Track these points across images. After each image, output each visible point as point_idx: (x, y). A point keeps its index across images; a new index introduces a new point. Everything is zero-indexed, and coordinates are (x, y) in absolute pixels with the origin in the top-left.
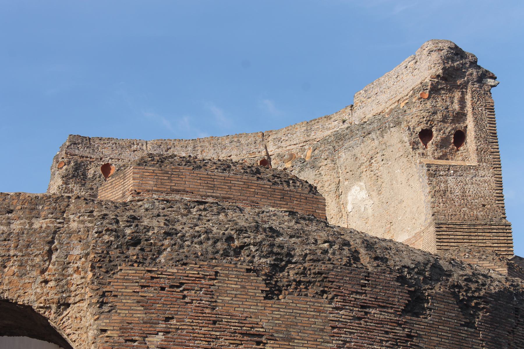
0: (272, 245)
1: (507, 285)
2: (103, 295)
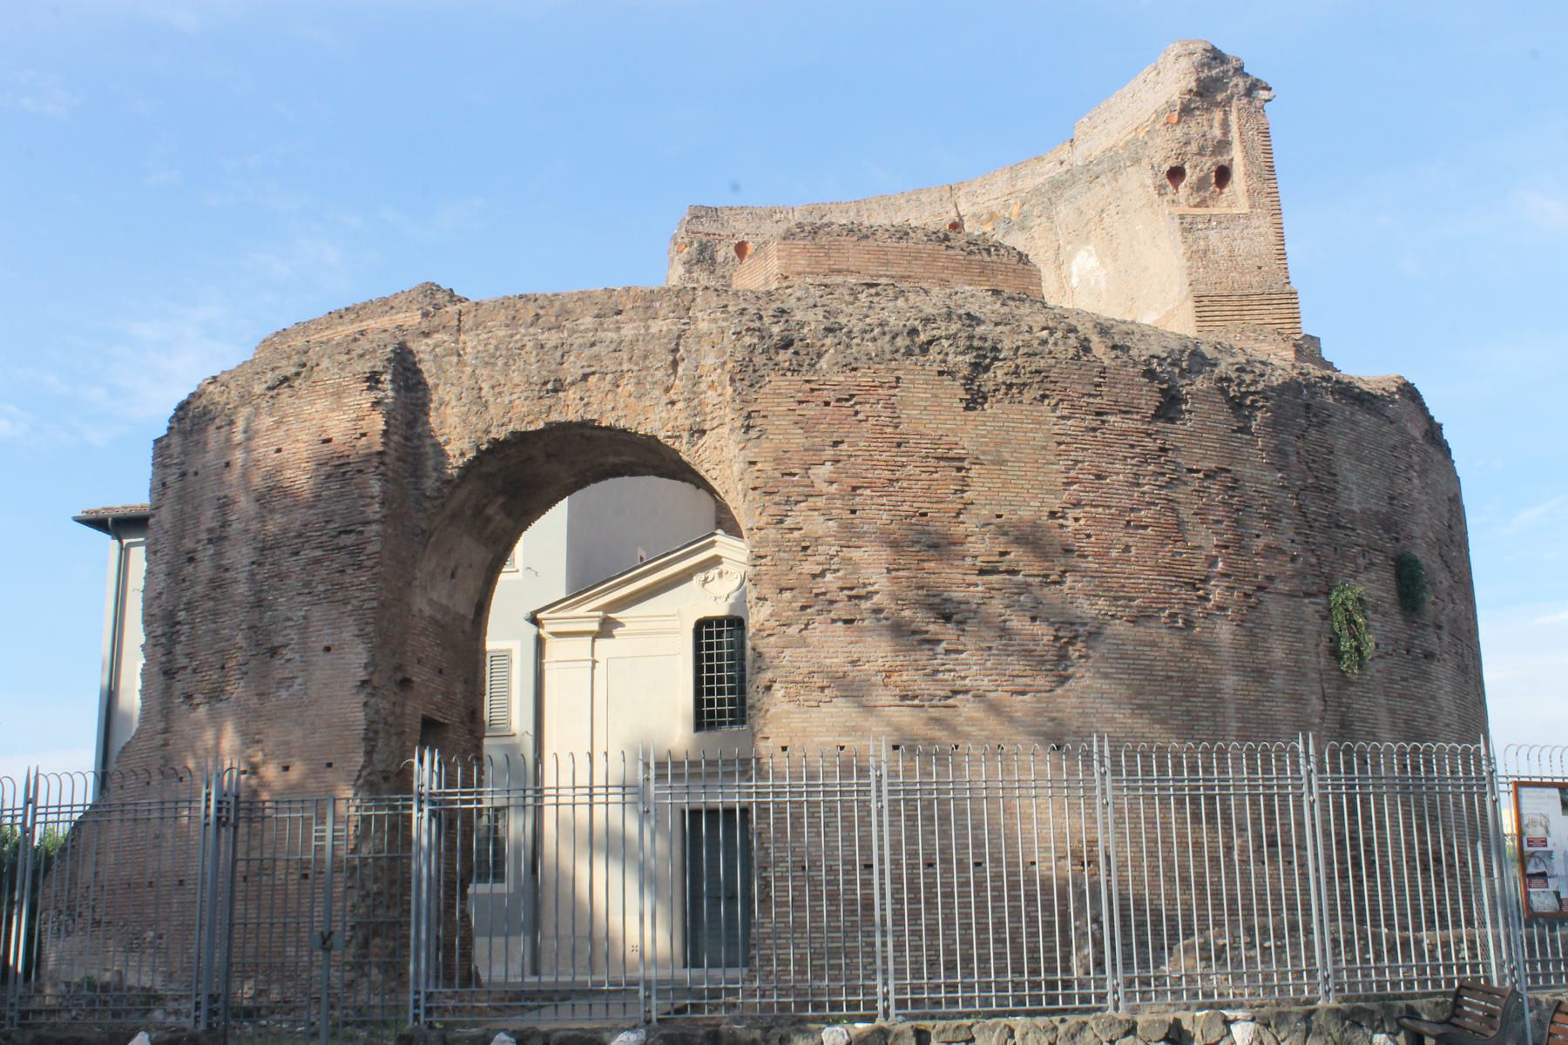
0: (971, 337)
1: (1294, 373)
2: (749, 416)
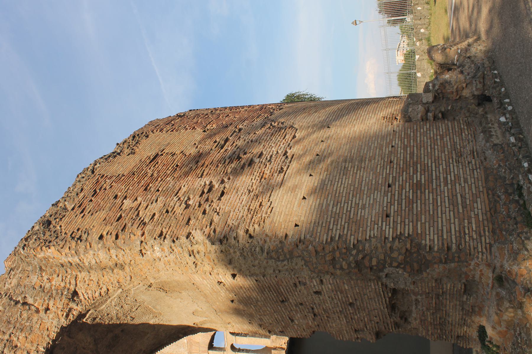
2: (73, 238)
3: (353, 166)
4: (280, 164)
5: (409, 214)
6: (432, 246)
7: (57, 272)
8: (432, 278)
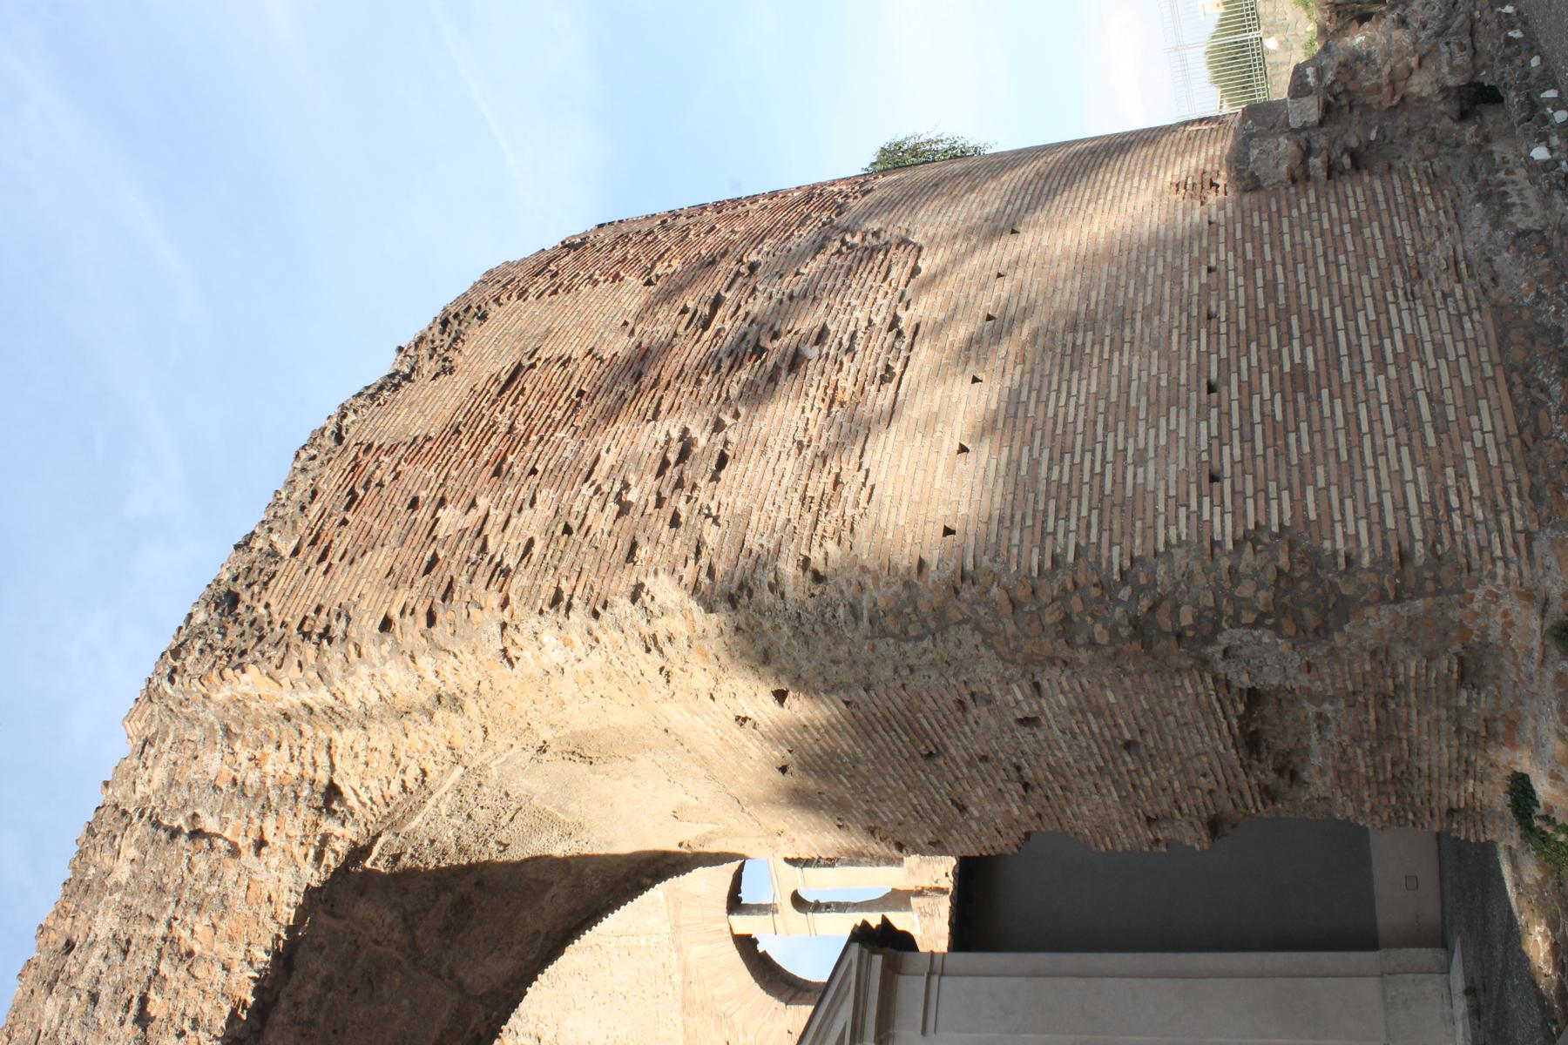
2: (306, 635)
3: (1098, 339)
4: (882, 356)
5: (1277, 468)
6: (1354, 553)
7: (275, 736)
8: (1362, 648)
